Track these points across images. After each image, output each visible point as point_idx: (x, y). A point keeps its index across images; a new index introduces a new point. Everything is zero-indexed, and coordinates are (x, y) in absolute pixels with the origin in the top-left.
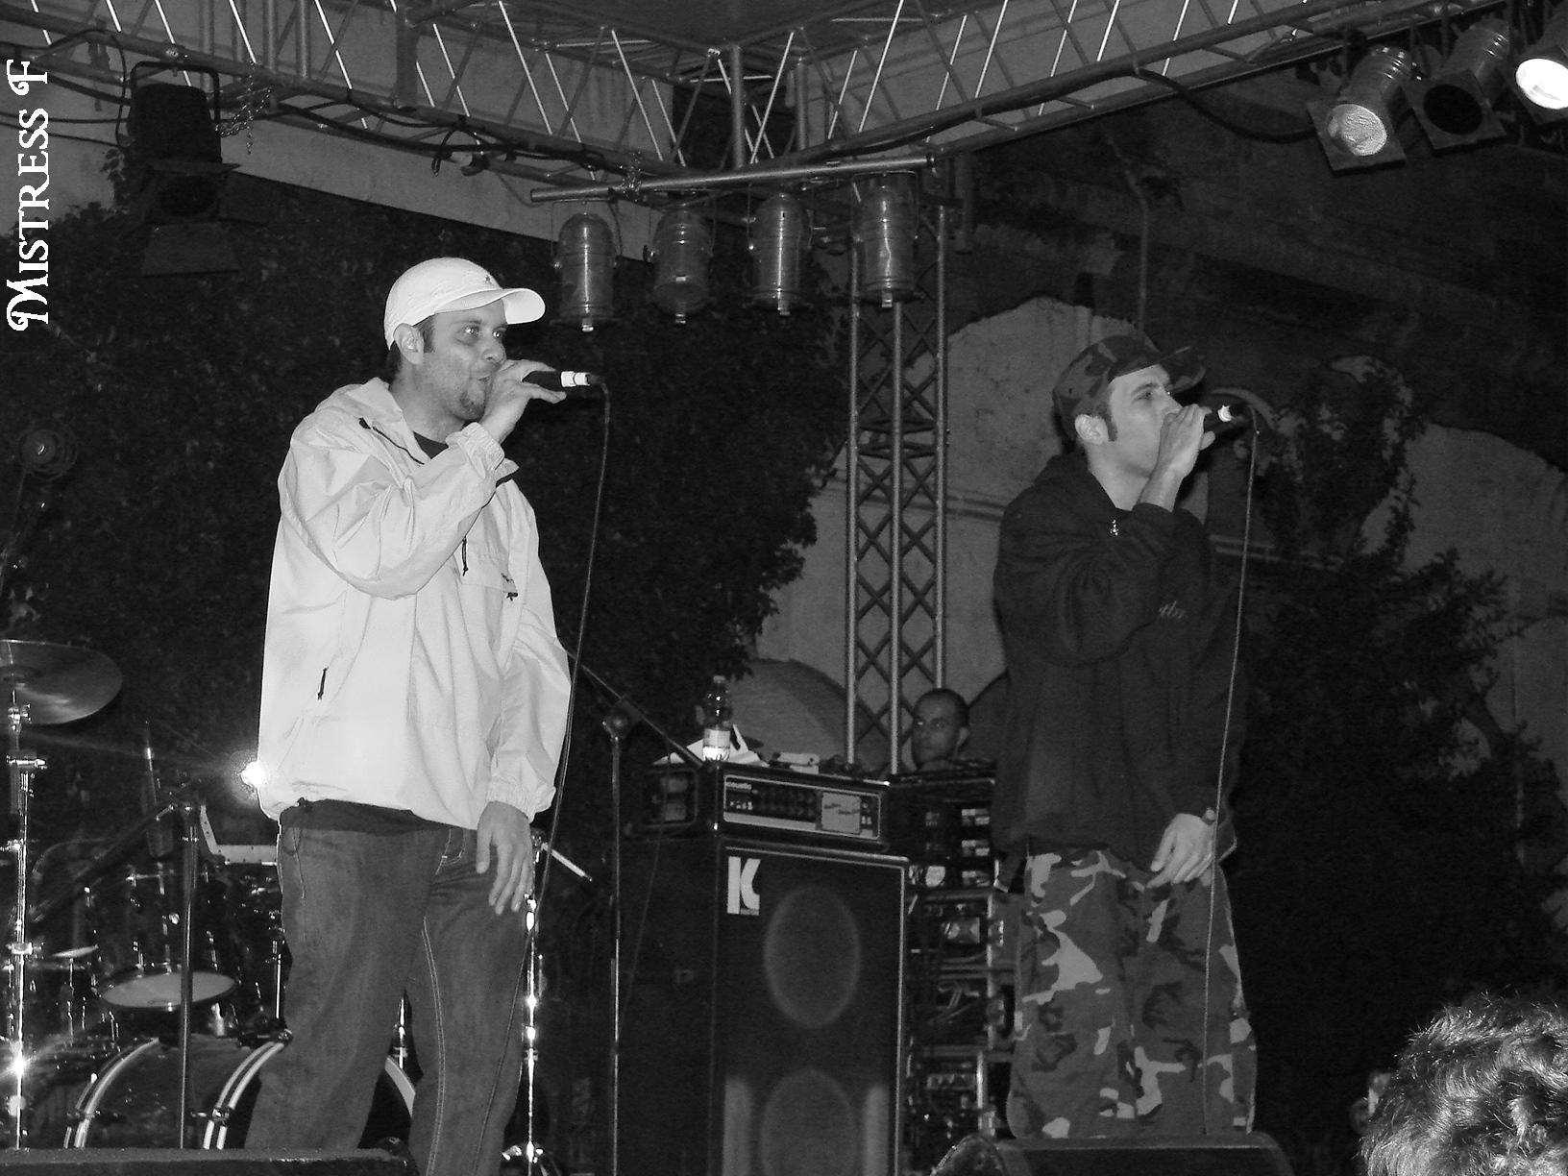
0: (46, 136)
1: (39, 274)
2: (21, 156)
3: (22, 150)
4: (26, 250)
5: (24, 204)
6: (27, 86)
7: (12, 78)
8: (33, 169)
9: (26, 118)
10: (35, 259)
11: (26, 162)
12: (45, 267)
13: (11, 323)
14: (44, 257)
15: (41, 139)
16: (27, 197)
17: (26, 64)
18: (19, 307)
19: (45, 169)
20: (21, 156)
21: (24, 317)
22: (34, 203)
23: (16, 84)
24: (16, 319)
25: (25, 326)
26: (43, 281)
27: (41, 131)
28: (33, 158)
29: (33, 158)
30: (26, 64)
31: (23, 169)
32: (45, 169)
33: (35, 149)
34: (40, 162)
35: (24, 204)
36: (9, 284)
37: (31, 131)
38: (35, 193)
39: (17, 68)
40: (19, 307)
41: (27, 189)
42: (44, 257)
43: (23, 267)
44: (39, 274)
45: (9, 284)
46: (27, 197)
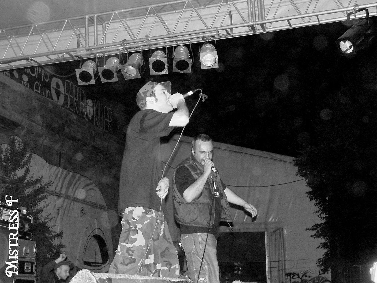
2: (10, 224)
3: (10, 223)
4: (11, 253)
5: (11, 239)
6: (11, 203)
7: (7, 201)
8: (13, 228)
10: (14, 255)
11: (11, 226)
12: (17, 258)
13: (7, 275)
14: (17, 255)
15: (15, 220)
16: (12, 236)
17: (11, 197)
19: (17, 228)
21: (11, 273)
22: (14, 238)
23: (8, 203)
24: (8, 273)
25: (11, 275)
28: (13, 225)
29: (13, 225)
30: (11, 197)
31: (10, 228)
32: (17, 228)
34: (16, 226)
35: (11, 239)
37: (12, 217)
38: (14, 235)
39: (9, 198)
41: (12, 234)
42: (17, 255)
43: (10, 258)
45: (6, 263)
46: (12, 236)
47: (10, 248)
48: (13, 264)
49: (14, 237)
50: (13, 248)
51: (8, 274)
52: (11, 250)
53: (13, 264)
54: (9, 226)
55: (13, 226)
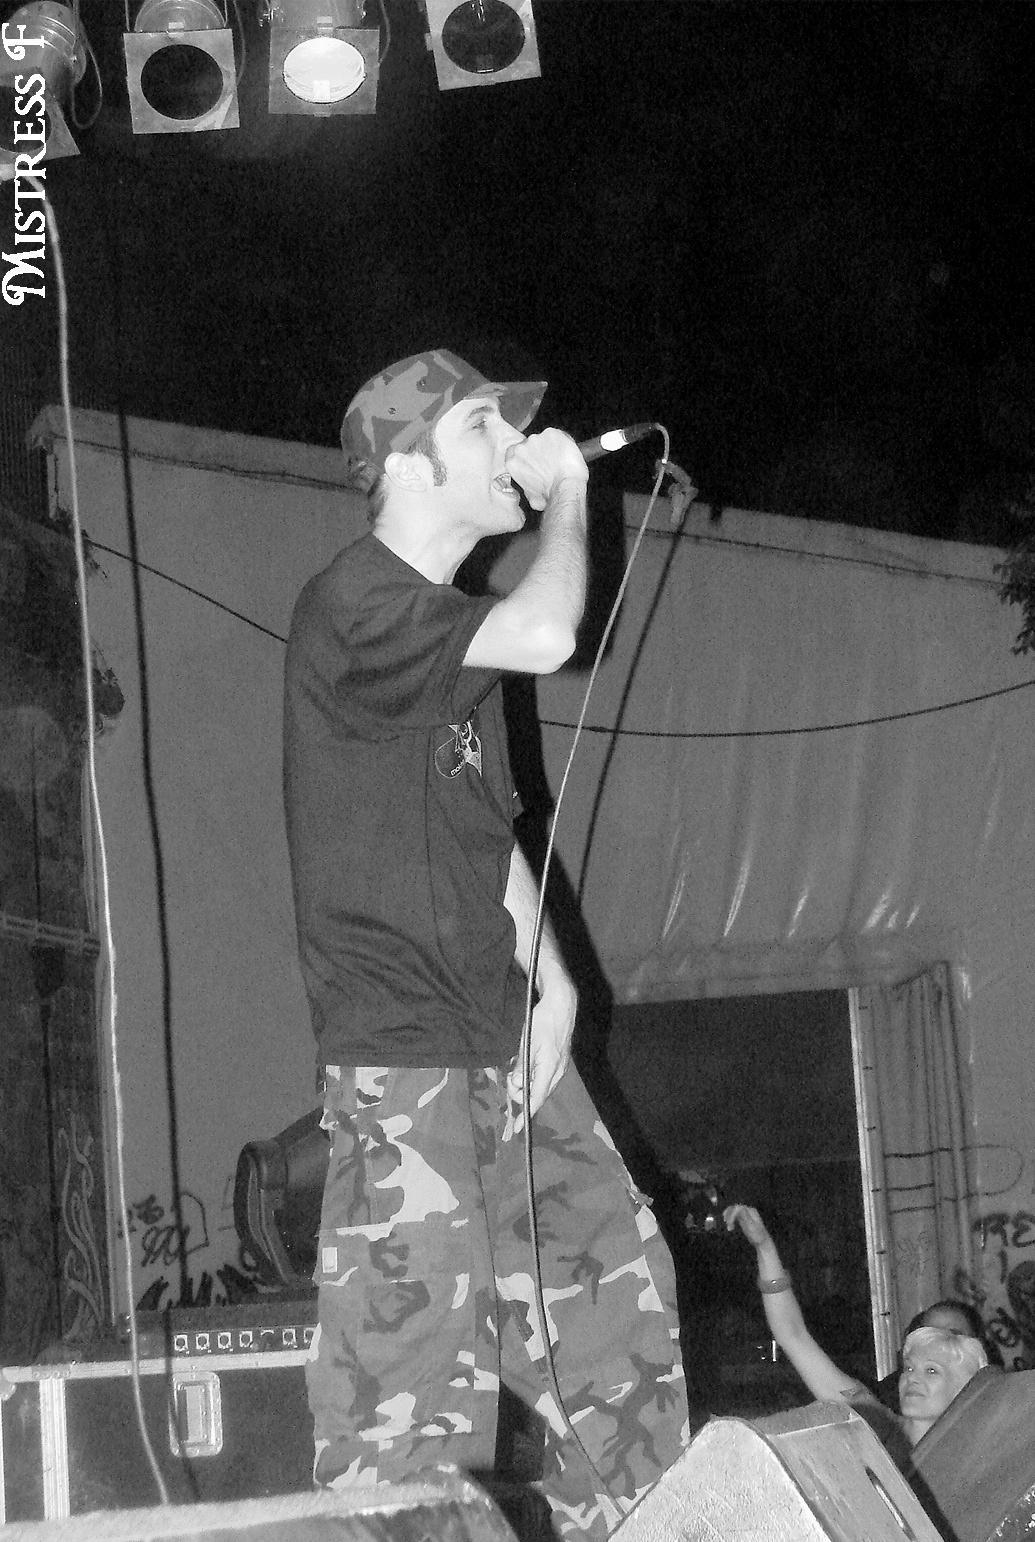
0: (43, 102)
1: (36, 246)
2: (17, 123)
3: (19, 117)
4: (22, 221)
6: (23, 50)
7: (7, 43)
8: (29, 137)
9: (22, 84)
10: (31, 231)
11: (23, 130)
13: (7, 297)
15: (37, 106)
17: (22, 28)
18: (15, 281)
20: (17, 123)
21: (20, 291)
23: (12, 48)
24: (11, 294)
25: (21, 300)
26: (40, 253)
27: (37, 98)
28: (30, 125)
29: (30, 125)
30: (22, 28)
31: (18, 137)
32: (41, 137)
33: (31, 116)
34: (37, 129)
36: (5, 257)
37: (27, 97)
38: (32, 162)
39: (13, 34)
40: (15, 281)
43: (19, 239)
44: (36, 246)
45: (5, 257)
47: (17, 207)
48: (30, 262)
49: (30, 168)
50: (29, 206)
51: (13, 297)
52: (21, 214)
53: (30, 262)
54: (16, 129)
55: (29, 130)
